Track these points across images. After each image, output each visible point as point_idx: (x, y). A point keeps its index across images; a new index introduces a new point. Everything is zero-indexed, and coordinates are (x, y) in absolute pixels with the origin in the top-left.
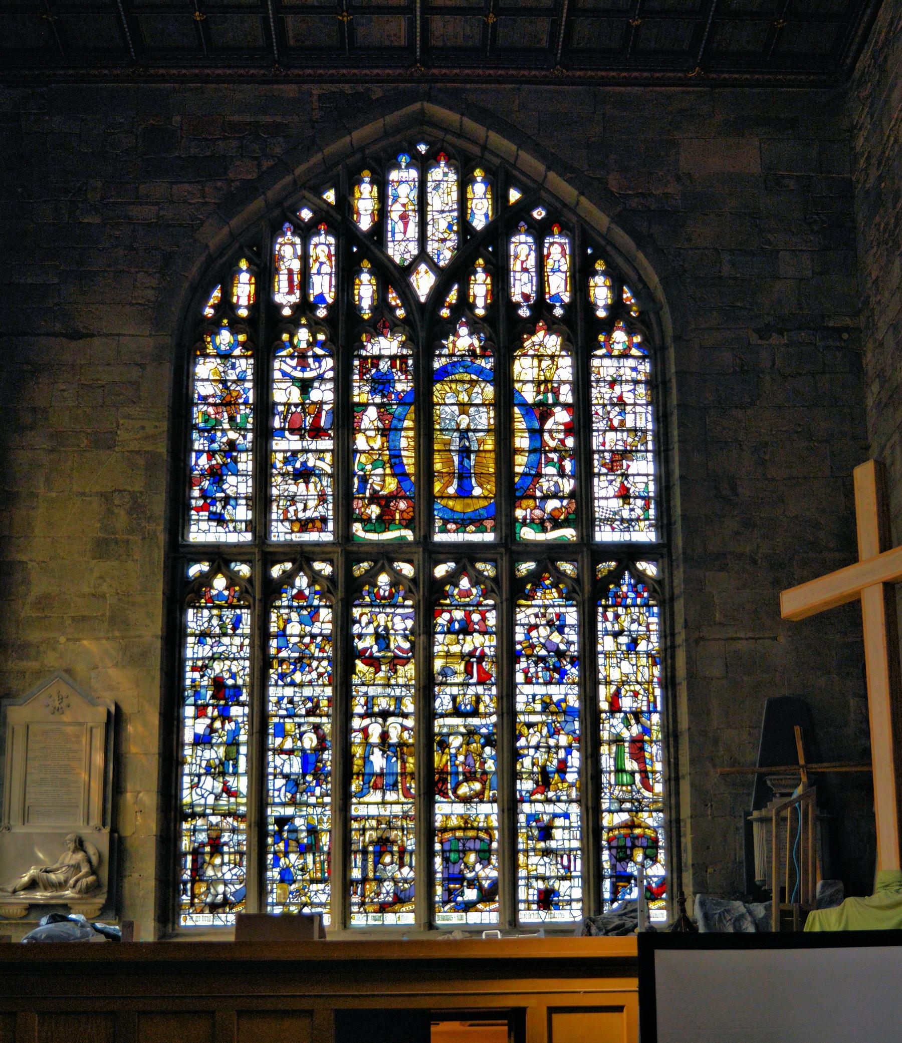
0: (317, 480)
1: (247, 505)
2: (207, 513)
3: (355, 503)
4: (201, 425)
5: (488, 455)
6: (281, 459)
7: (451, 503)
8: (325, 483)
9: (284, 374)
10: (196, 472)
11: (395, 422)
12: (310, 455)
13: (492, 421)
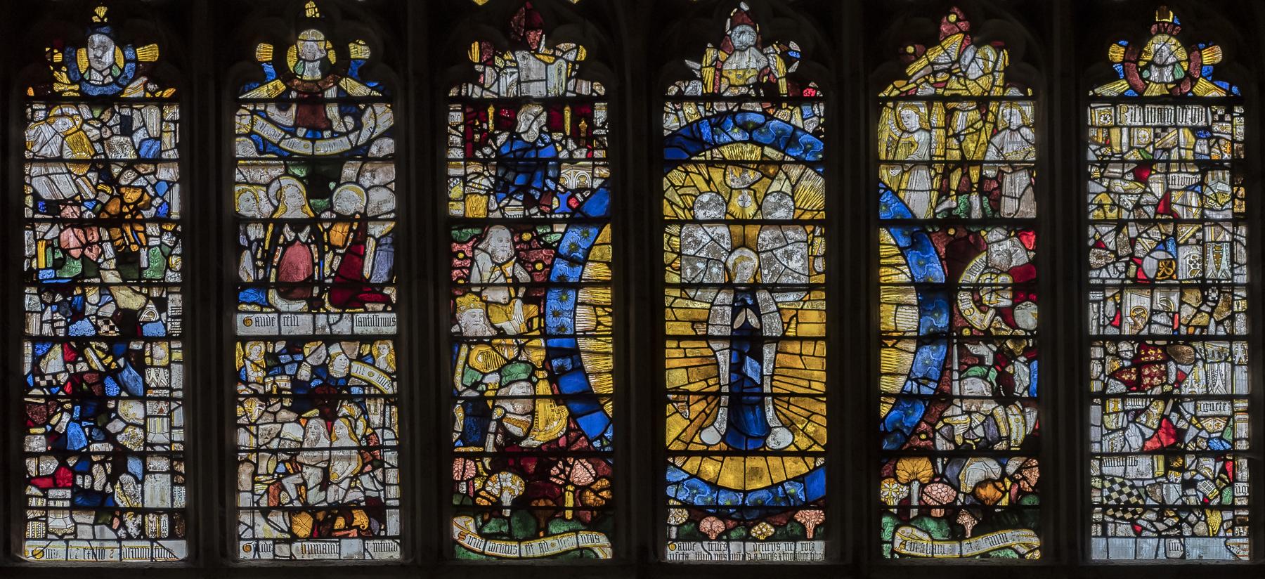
0: (356, 411)
1: (172, 472)
2: (68, 493)
3: (458, 465)
4: (46, 275)
5: (808, 348)
6: (261, 360)
7: (710, 468)
8: (376, 420)
9: (264, 146)
10: (36, 392)
11: (561, 267)
12: (335, 349)
13: (820, 265)
